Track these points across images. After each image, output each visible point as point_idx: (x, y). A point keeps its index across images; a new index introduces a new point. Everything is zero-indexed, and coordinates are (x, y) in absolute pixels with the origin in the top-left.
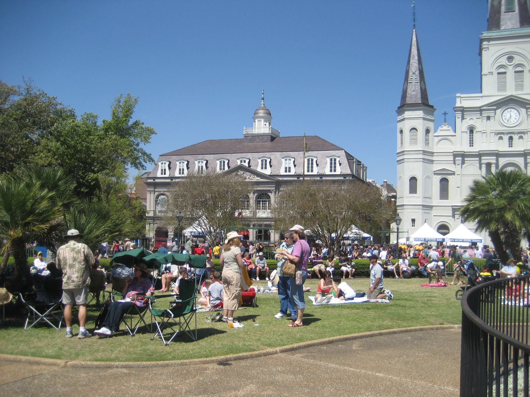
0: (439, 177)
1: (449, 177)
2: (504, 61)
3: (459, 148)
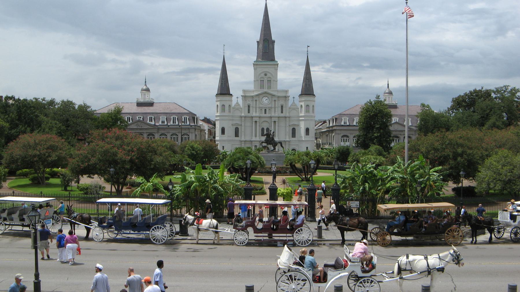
0: (235, 127)
1: (239, 127)
2: (263, 75)
3: (243, 115)
